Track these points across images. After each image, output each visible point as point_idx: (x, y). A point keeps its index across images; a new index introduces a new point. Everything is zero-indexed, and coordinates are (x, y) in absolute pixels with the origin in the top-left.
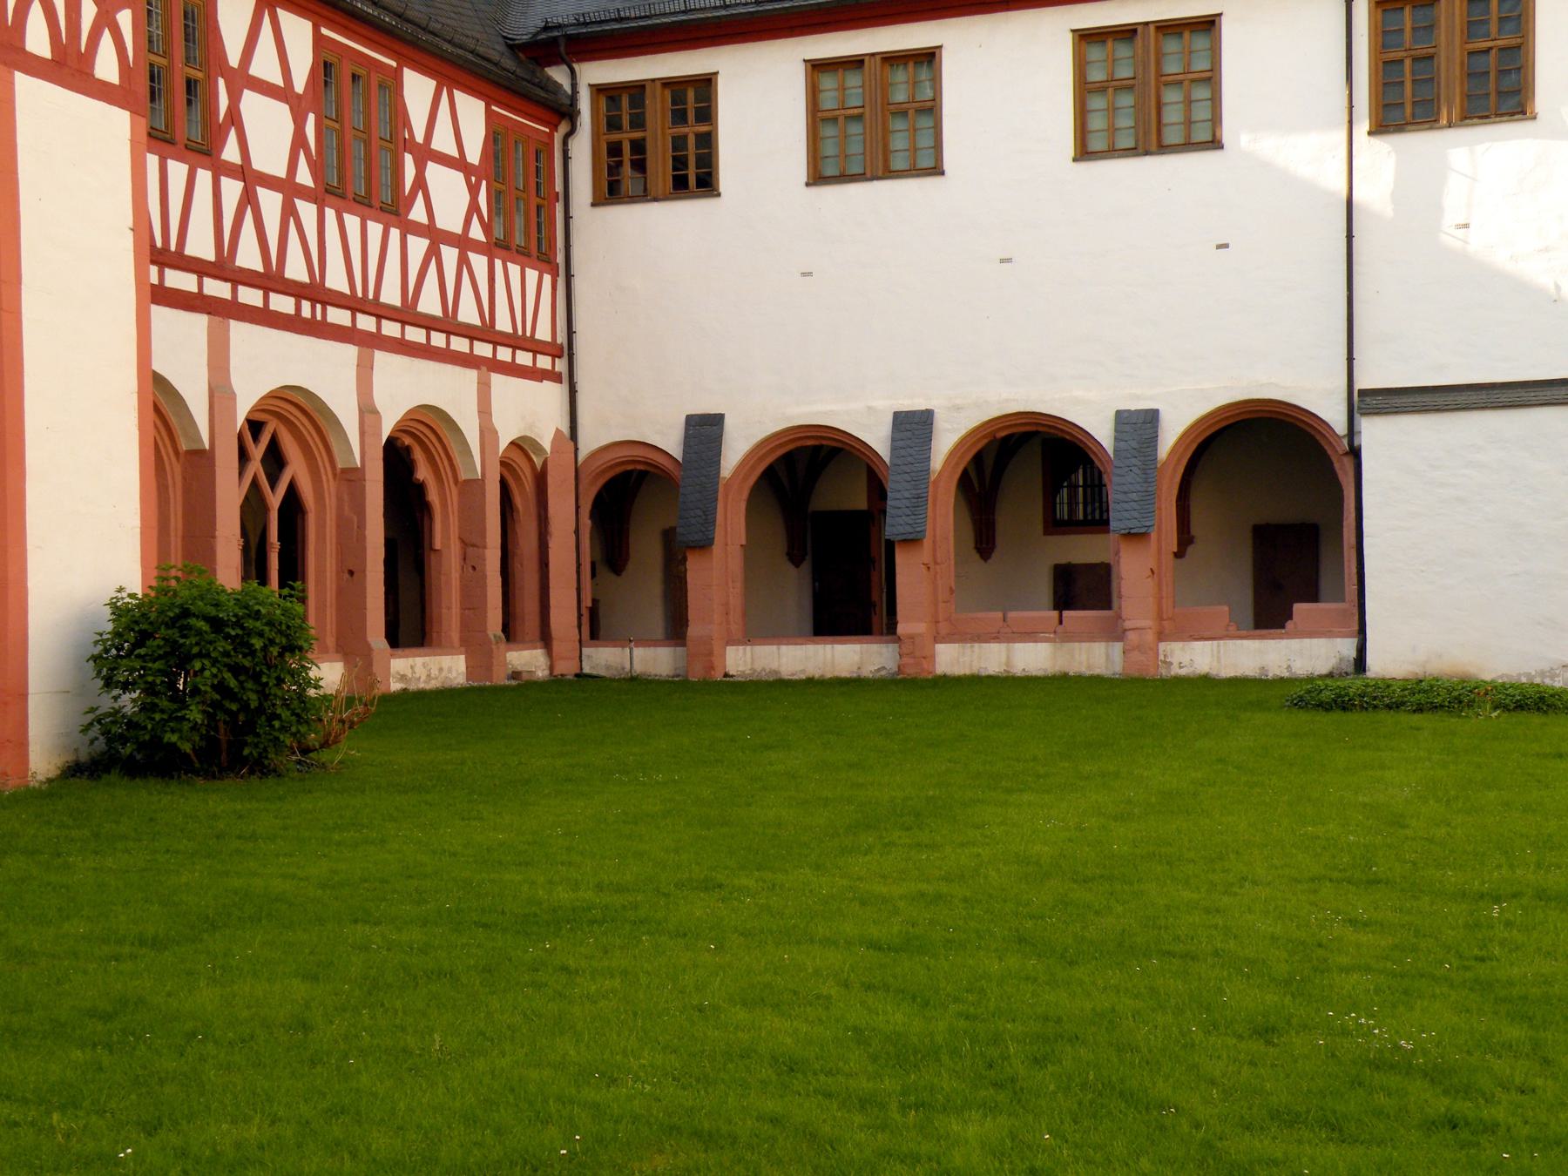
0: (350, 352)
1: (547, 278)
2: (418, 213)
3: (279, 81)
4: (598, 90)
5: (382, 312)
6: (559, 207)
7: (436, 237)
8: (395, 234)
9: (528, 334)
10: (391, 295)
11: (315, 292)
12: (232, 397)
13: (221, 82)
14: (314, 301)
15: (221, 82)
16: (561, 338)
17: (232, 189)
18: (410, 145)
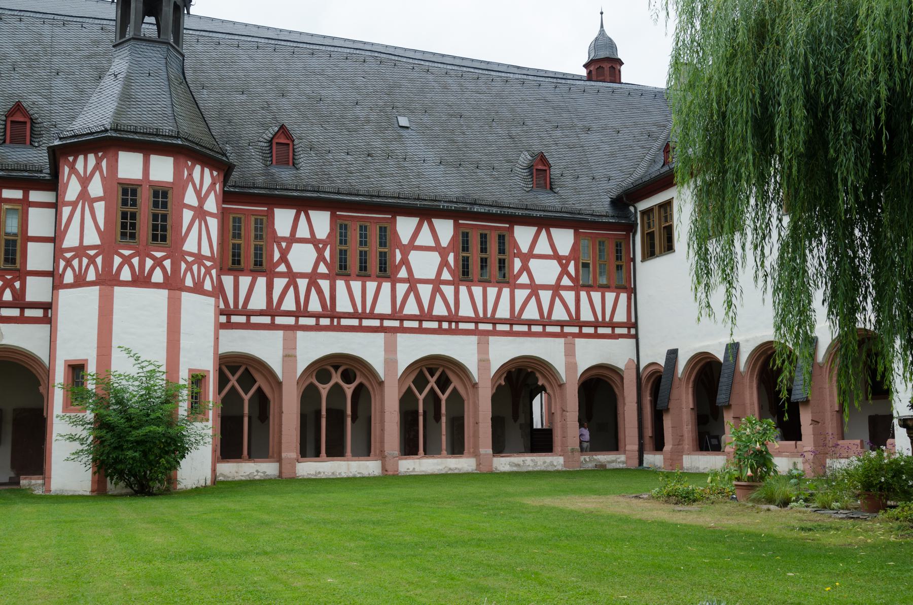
1: (623, 297)
2: (524, 279)
3: (432, 244)
4: (644, 213)
5: (495, 322)
6: (632, 263)
7: (534, 289)
9: (607, 319)
11: (454, 318)
12: (396, 361)
13: (398, 251)
14: (450, 322)
15: (398, 251)
16: (633, 320)
17: (402, 288)
18: (520, 254)
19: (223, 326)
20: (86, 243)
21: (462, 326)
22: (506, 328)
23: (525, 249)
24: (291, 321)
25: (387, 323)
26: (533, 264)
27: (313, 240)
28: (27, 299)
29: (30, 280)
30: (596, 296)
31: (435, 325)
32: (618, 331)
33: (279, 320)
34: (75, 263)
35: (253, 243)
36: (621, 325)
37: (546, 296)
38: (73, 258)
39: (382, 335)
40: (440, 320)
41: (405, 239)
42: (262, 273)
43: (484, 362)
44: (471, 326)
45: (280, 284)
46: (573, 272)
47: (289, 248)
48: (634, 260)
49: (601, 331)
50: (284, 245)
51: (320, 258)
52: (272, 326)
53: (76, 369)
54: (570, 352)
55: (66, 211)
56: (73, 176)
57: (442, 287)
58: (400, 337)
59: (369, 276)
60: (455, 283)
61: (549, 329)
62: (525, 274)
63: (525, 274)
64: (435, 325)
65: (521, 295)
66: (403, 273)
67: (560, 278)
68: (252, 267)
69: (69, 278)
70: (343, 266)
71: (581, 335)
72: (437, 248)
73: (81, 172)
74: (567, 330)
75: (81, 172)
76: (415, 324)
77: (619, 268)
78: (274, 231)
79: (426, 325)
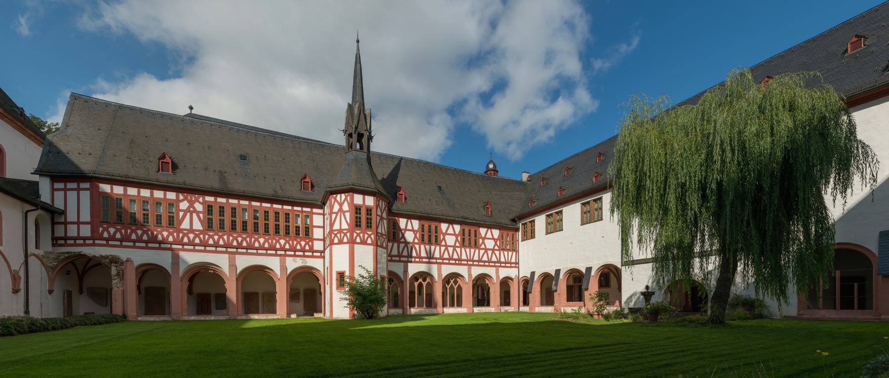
0: (467, 267)
1: (514, 253)
3: (453, 233)
5: (473, 261)
7: (486, 250)
8: (477, 251)
9: (509, 261)
10: (476, 258)
11: (460, 259)
16: (517, 261)
17: (443, 249)
19: (389, 261)
20: (342, 228)
21: (463, 262)
22: (477, 263)
23: (483, 236)
24: (406, 259)
25: (438, 261)
26: (486, 241)
27: (413, 230)
28: (314, 249)
29: (315, 242)
30: (506, 253)
31: (454, 262)
32: (512, 265)
33: (402, 259)
34: (339, 235)
35: (392, 230)
36: (513, 263)
37: (490, 252)
38: (337, 233)
39: (437, 265)
40: (456, 260)
41: (444, 231)
42: (396, 241)
43: (470, 275)
44: (466, 262)
45: (402, 246)
46: (499, 245)
47: (405, 232)
48: (518, 241)
49: (507, 265)
50: (403, 232)
51: (415, 237)
52: (400, 261)
53: (341, 275)
54: (497, 272)
55: (334, 216)
56: (336, 203)
57: (456, 248)
58: (442, 266)
59: (432, 244)
60: (460, 247)
61: (491, 264)
62: (483, 245)
63: (483, 245)
64: (454, 262)
65: (482, 252)
66: (443, 243)
67: (494, 247)
68: (392, 239)
69: (336, 241)
70: (423, 240)
71: (501, 266)
72: (454, 234)
73: (339, 201)
74: (496, 264)
75: (339, 201)
76: (447, 261)
77: (513, 243)
78: (399, 227)
79: (451, 262)
